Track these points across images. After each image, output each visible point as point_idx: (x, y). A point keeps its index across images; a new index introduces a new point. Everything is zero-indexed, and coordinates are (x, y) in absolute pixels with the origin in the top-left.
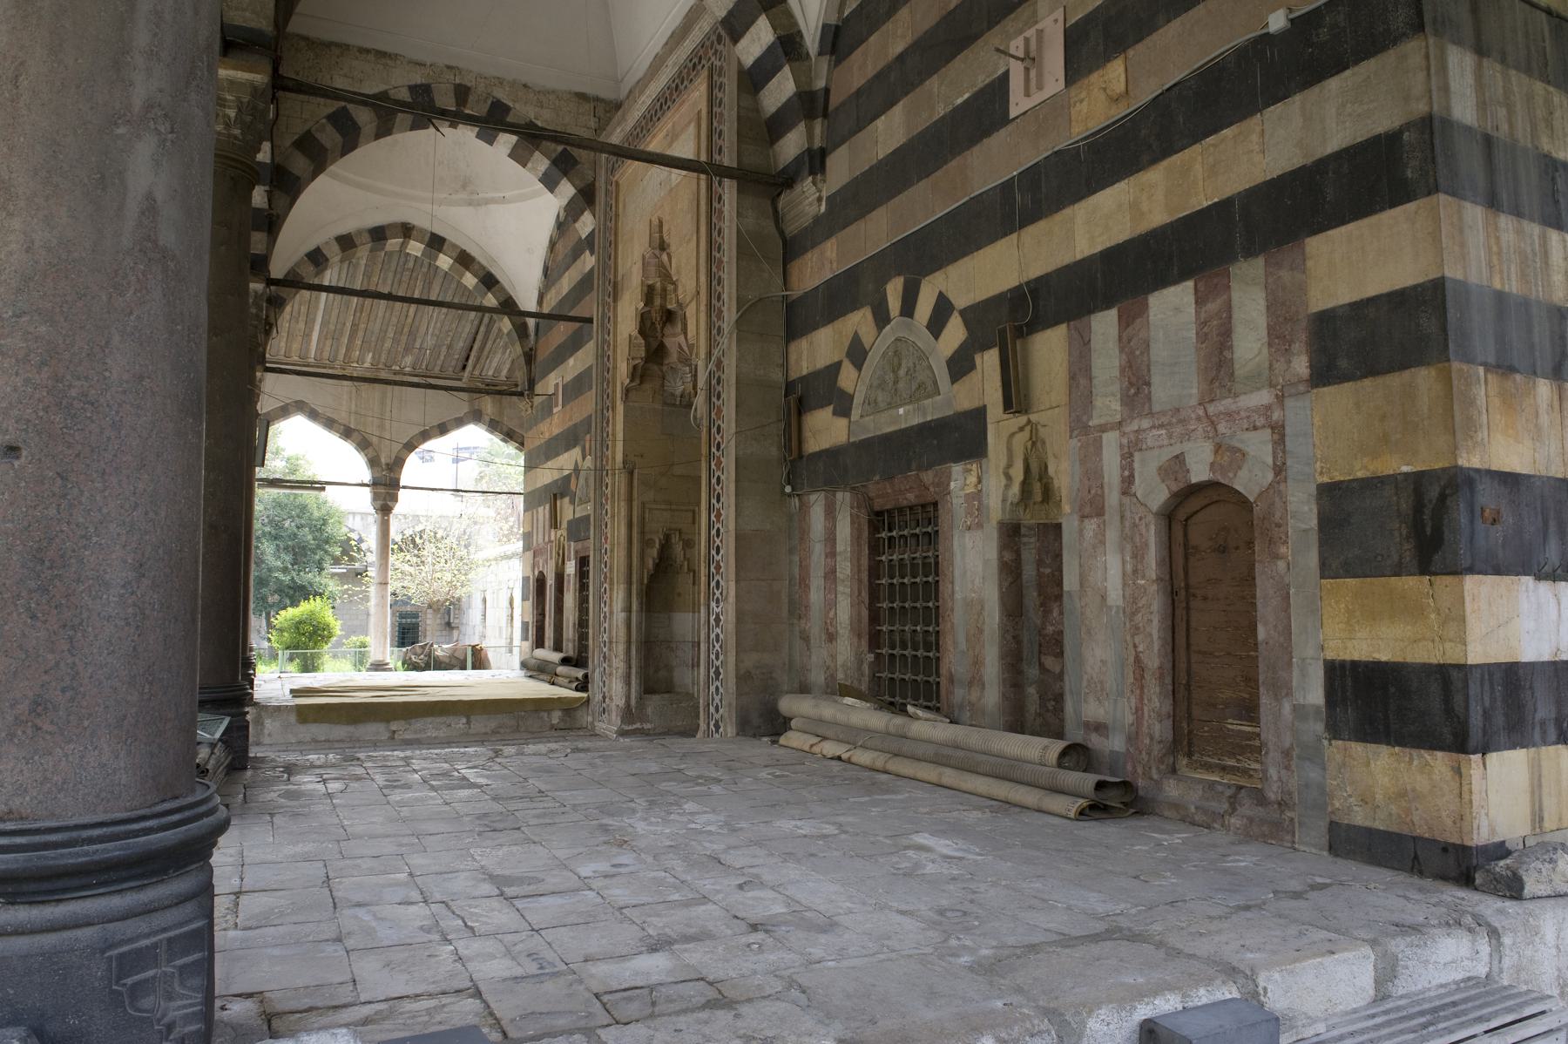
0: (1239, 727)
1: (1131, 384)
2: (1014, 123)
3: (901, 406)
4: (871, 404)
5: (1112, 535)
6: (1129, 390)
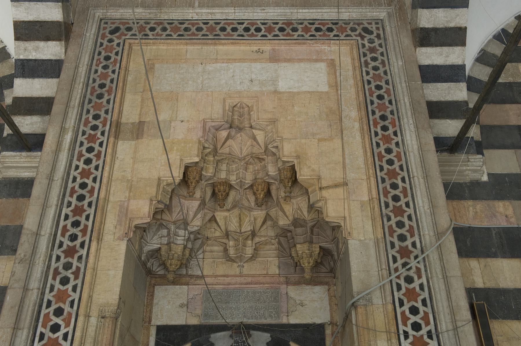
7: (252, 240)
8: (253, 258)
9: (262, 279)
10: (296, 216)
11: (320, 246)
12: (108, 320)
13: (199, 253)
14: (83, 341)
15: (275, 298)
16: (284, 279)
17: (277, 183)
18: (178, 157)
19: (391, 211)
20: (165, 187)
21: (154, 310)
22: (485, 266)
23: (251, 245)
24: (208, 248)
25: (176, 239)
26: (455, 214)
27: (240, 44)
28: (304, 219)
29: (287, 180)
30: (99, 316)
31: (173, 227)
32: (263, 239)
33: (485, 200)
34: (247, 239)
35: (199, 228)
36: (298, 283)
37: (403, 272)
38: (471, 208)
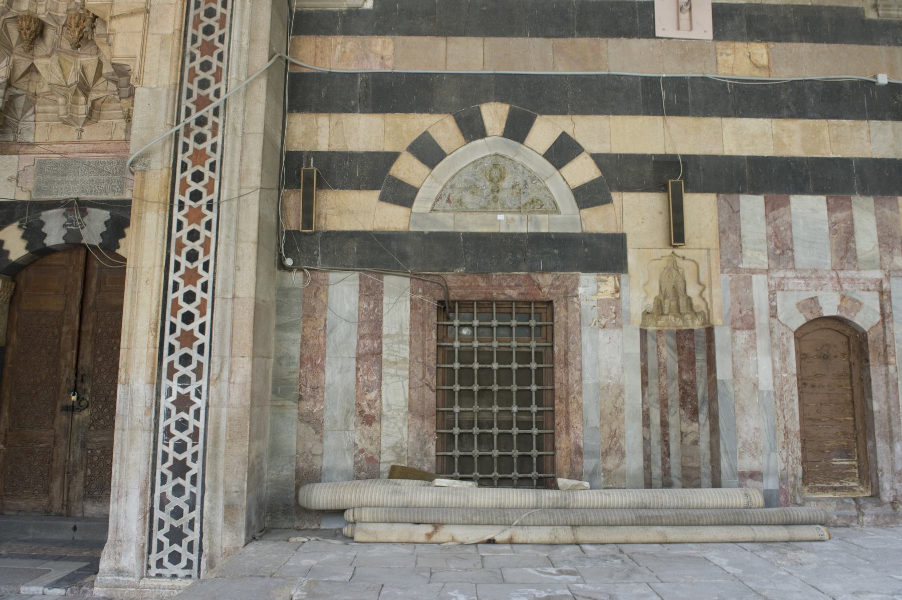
0: (840, 463)
1: (777, 247)
2: (658, 41)
3: (502, 212)
4: (444, 199)
5: (762, 342)
6: (775, 250)
7: (86, 96)
9: (105, 147)
13: (28, 114)
15: (120, 171)
19: (198, 48)
22: (337, 123)
24: (40, 107)
26: (316, 55)
32: (102, 94)
33: (361, 35)
37: (206, 130)
38: (339, 47)
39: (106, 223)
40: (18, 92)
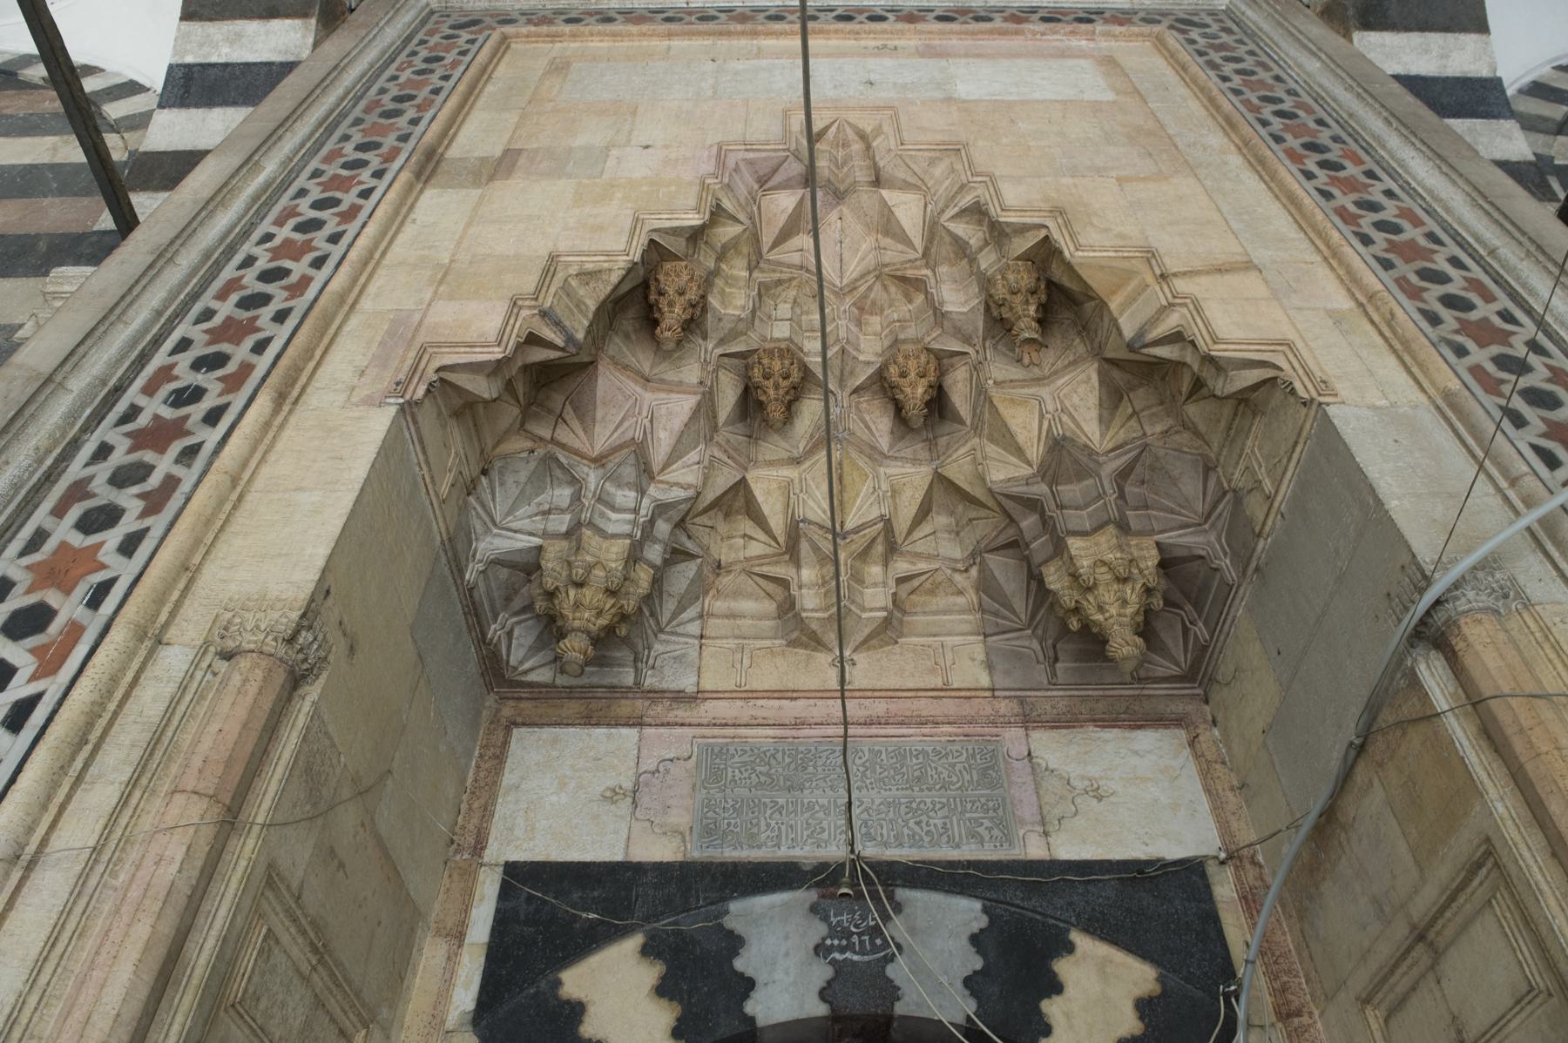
8: (889, 629)
9: (925, 707)
10: (1058, 431)
11: (1158, 544)
12: (244, 663)
13: (685, 616)
14: (94, 736)
15: (984, 773)
16: (1014, 707)
17: (970, 350)
18: (630, 212)
20: (574, 283)
21: (502, 808)
23: (880, 579)
24: (718, 604)
25: (602, 515)
27: (828, 32)
28: (1086, 446)
29: (1018, 299)
30: (207, 643)
31: (592, 478)
32: (922, 566)
34: (864, 555)
35: (691, 493)
36: (1065, 722)
39: (975, 939)
40: (690, 546)
